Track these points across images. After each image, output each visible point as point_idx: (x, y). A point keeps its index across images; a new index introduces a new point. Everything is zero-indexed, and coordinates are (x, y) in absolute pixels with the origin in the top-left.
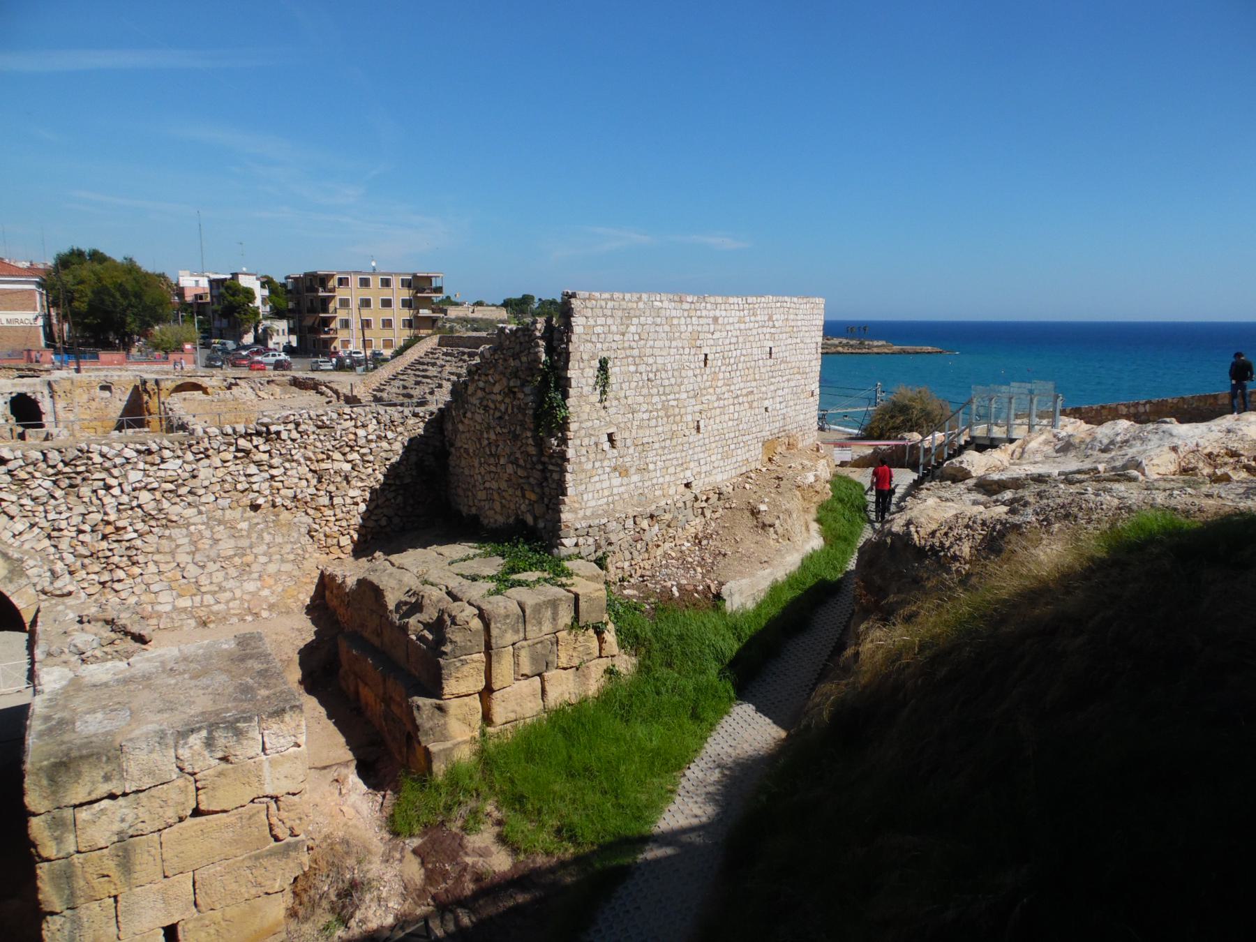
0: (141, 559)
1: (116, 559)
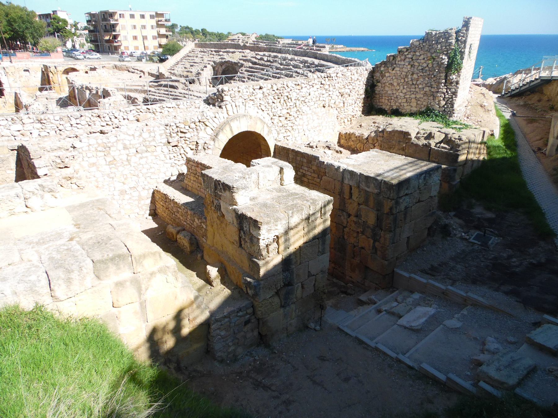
1: (288, 128)
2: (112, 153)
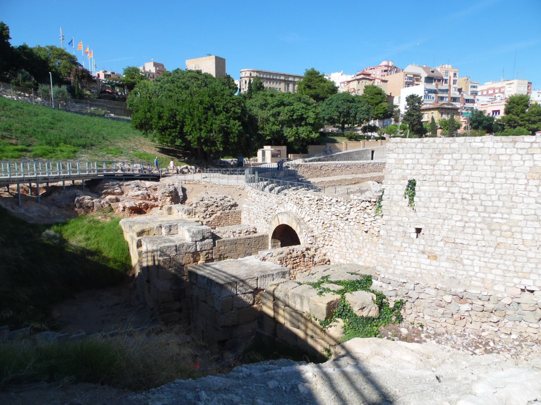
0: (332, 239)
2: (250, 215)
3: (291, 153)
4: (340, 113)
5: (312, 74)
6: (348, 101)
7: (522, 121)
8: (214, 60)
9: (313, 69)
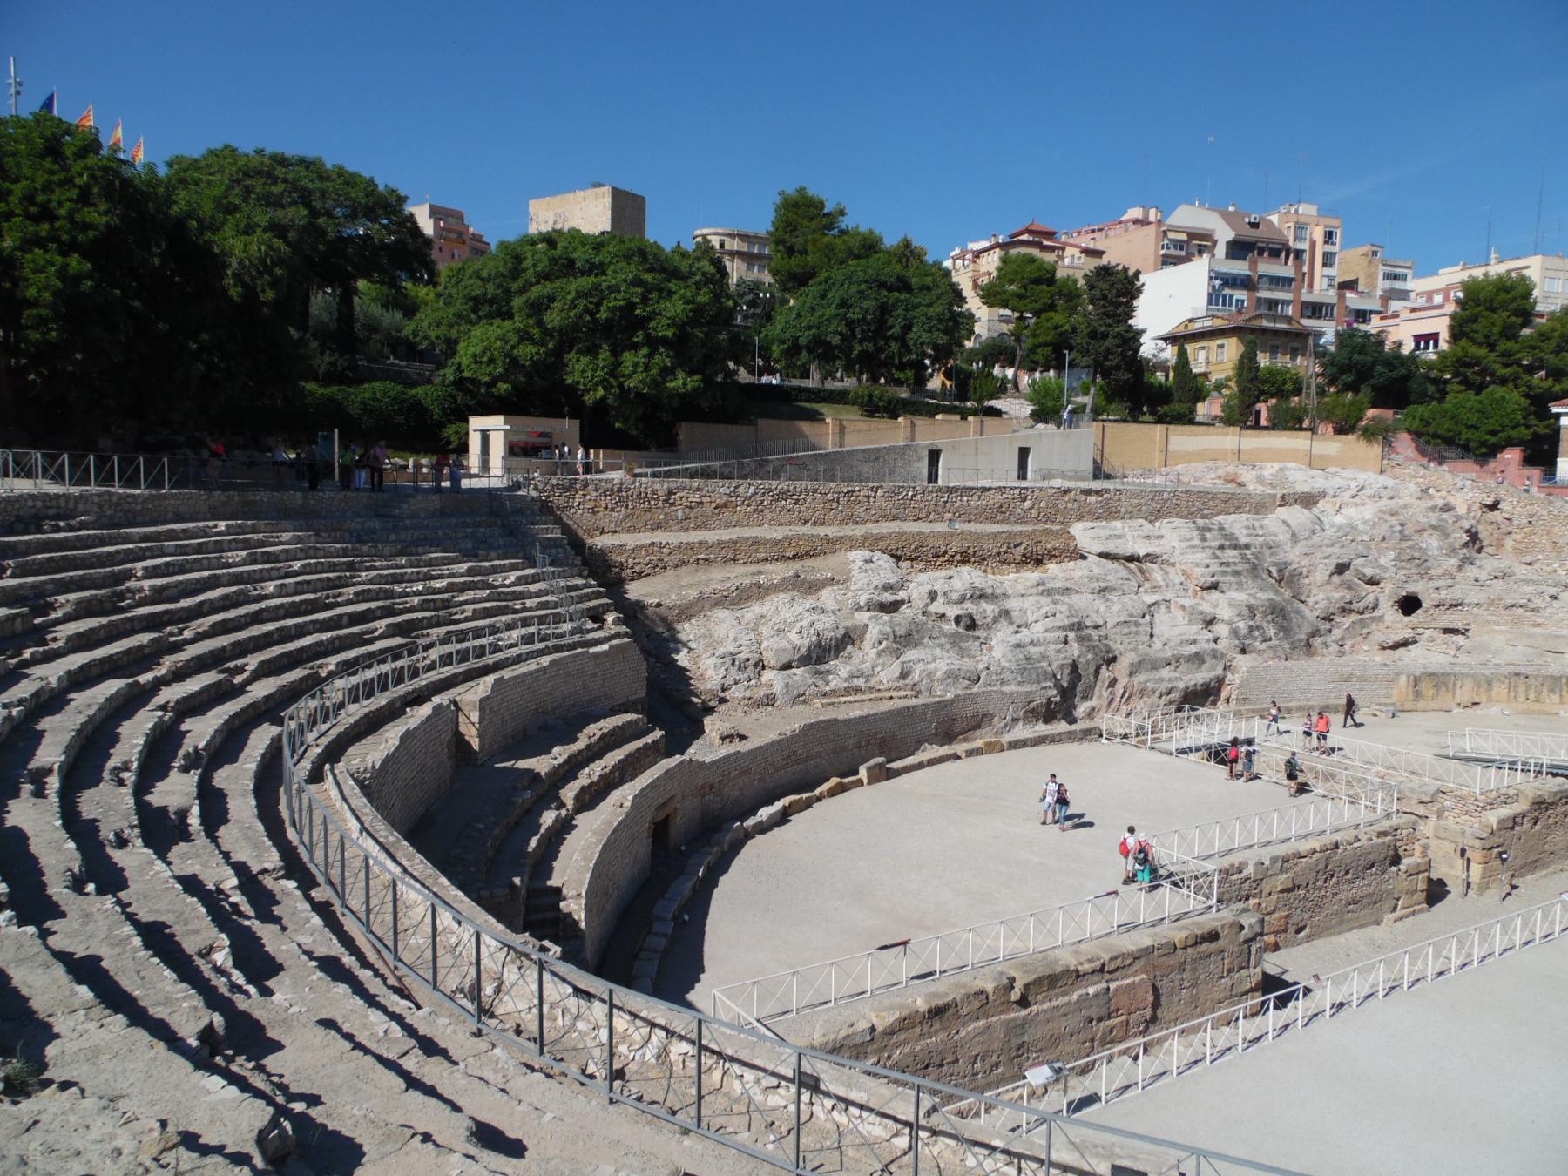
3: (597, 447)
4: (851, 324)
5: (796, 205)
6: (882, 285)
7: (1506, 366)
8: (608, 200)
9: (802, 191)
